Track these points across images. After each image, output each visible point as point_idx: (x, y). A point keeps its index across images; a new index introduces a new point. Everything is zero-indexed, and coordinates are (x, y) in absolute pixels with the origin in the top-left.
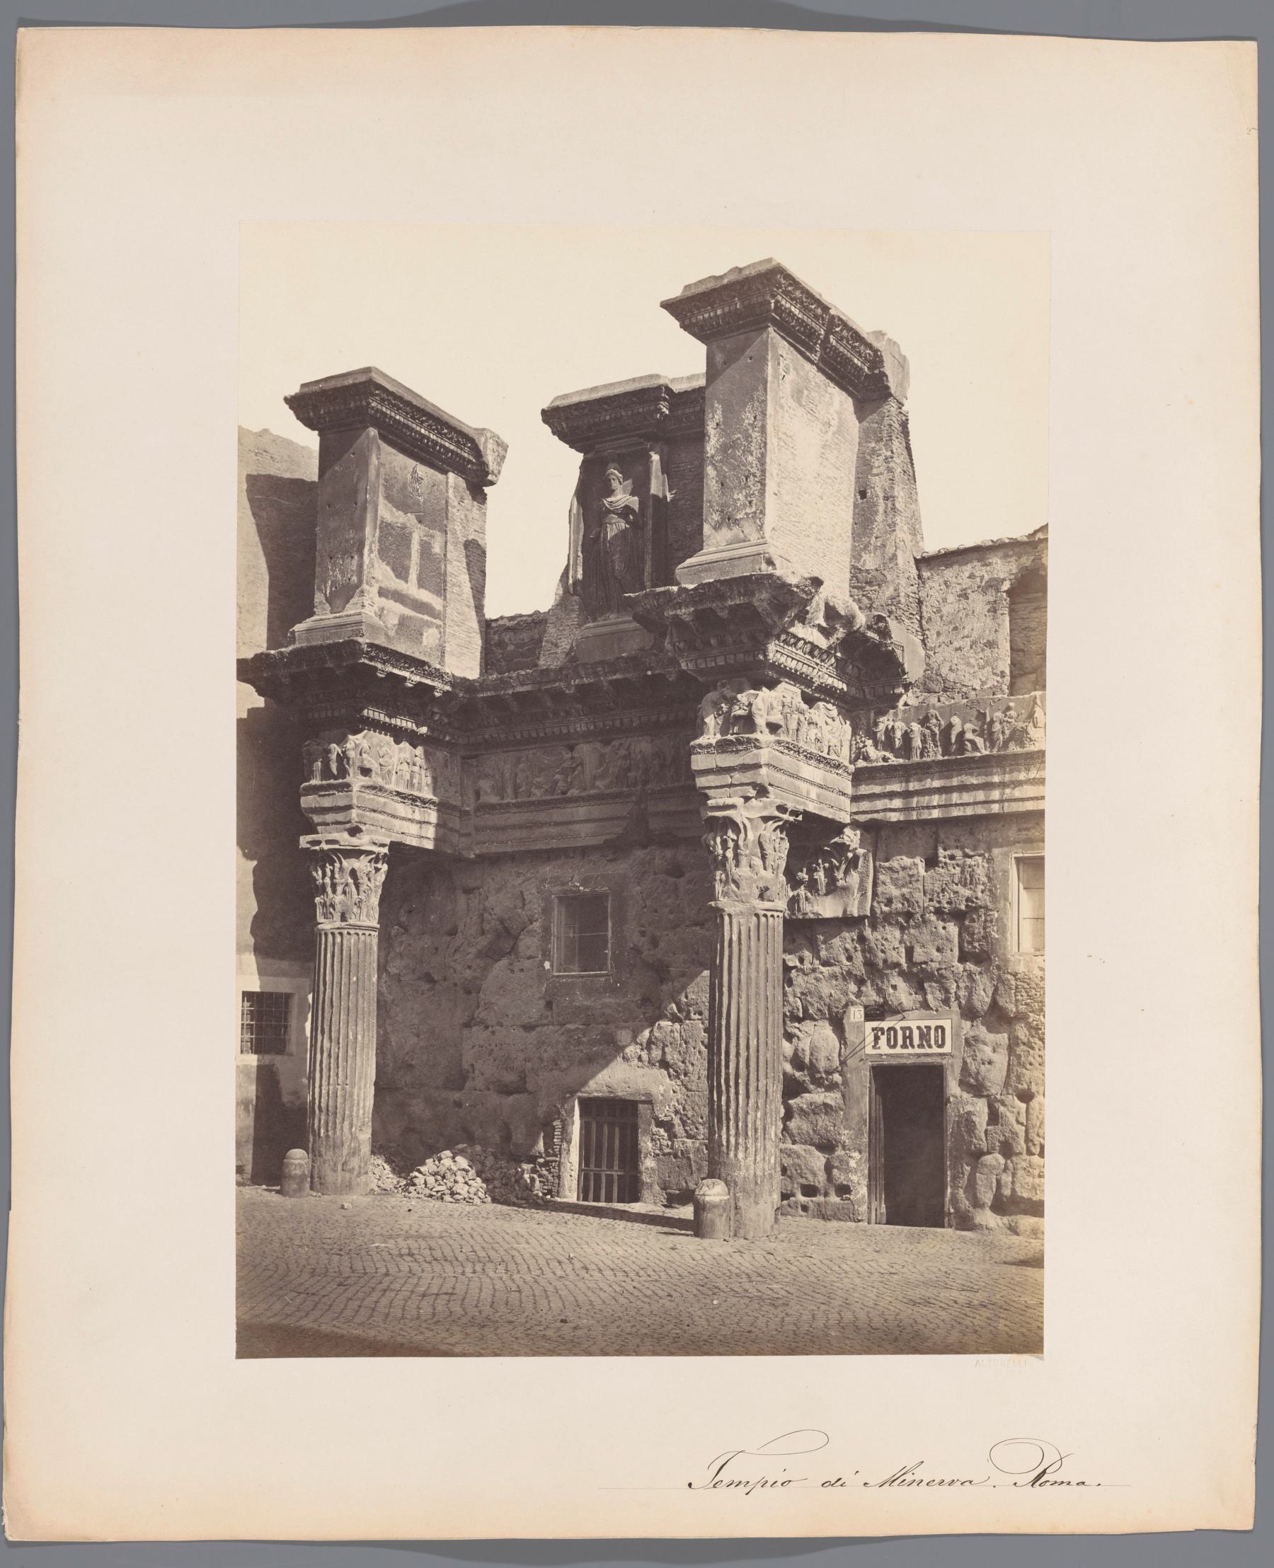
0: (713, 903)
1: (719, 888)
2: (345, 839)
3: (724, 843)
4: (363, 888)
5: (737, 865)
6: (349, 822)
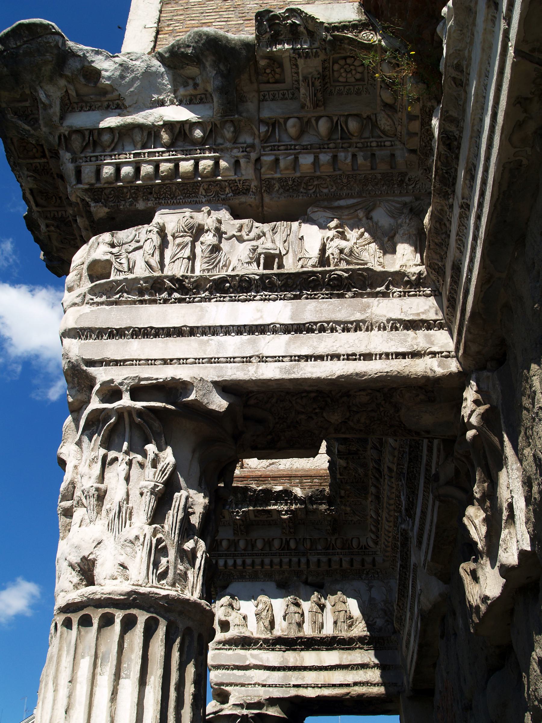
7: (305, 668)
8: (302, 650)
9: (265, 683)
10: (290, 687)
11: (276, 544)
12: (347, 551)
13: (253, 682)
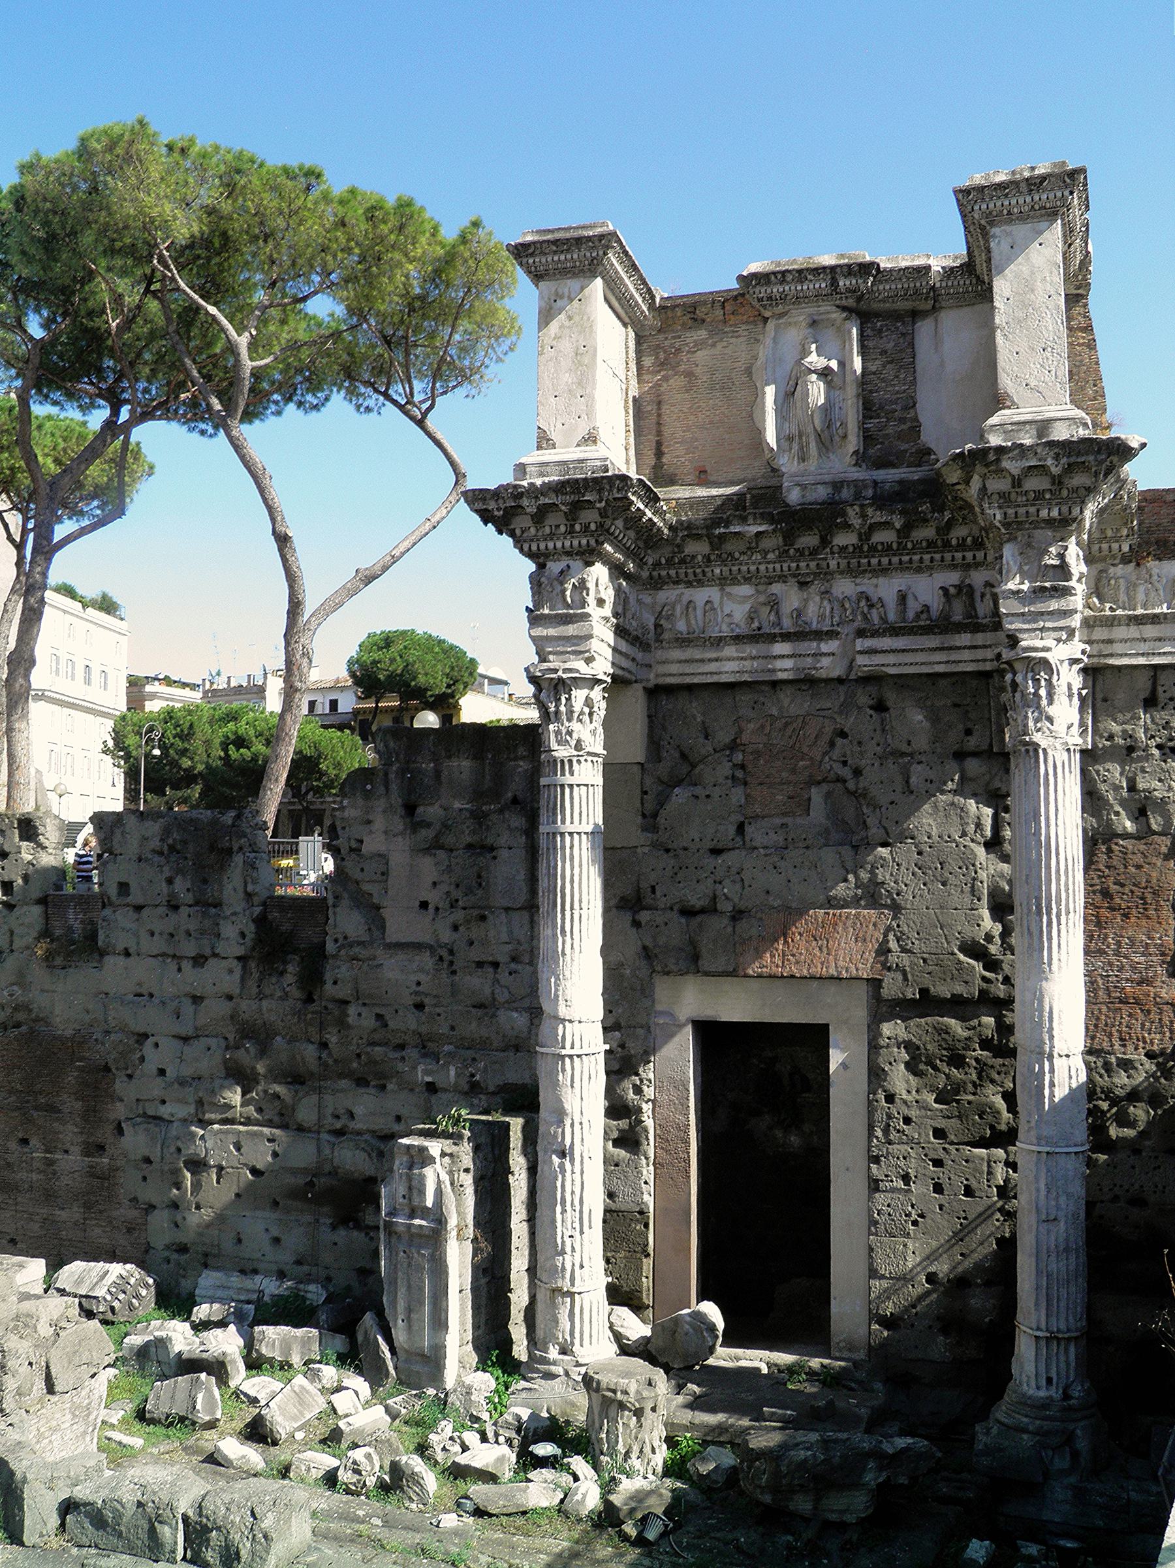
0: (1027, 739)
1: (1031, 724)
3: (1037, 682)
5: (1051, 703)
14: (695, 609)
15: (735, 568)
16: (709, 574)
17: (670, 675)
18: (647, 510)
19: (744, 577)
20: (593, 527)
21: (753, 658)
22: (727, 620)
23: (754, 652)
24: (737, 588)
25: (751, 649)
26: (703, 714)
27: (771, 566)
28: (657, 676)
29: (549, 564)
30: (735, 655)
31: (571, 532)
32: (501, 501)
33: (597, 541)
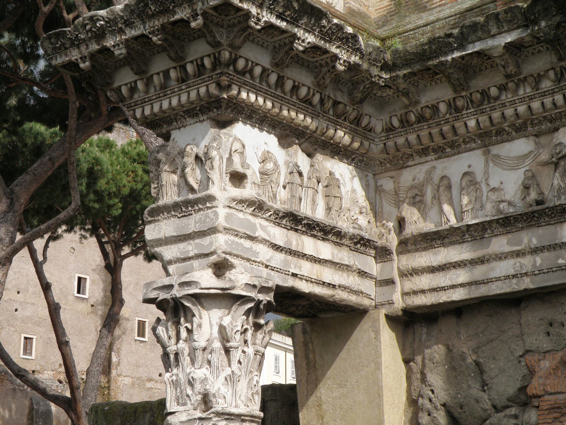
2: (206, 279)
4: (236, 355)
6: (212, 253)
7: (303, 256)
8: (303, 233)
9: (268, 264)
10: (288, 275)
11: (303, 92)
12: (353, 126)
13: (258, 260)
14: (449, 187)
15: (496, 115)
16: (462, 130)
17: (423, 292)
18: (300, 33)
19: (512, 125)
20: (207, 62)
21: (535, 251)
22: (494, 197)
23: (535, 242)
24: (507, 145)
25: (530, 238)
26: (475, 351)
27: (548, 101)
28: (405, 294)
29: (175, 134)
30: (507, 249)
31: (183, 79)
32: (83, 48)
33: (219, 85)
